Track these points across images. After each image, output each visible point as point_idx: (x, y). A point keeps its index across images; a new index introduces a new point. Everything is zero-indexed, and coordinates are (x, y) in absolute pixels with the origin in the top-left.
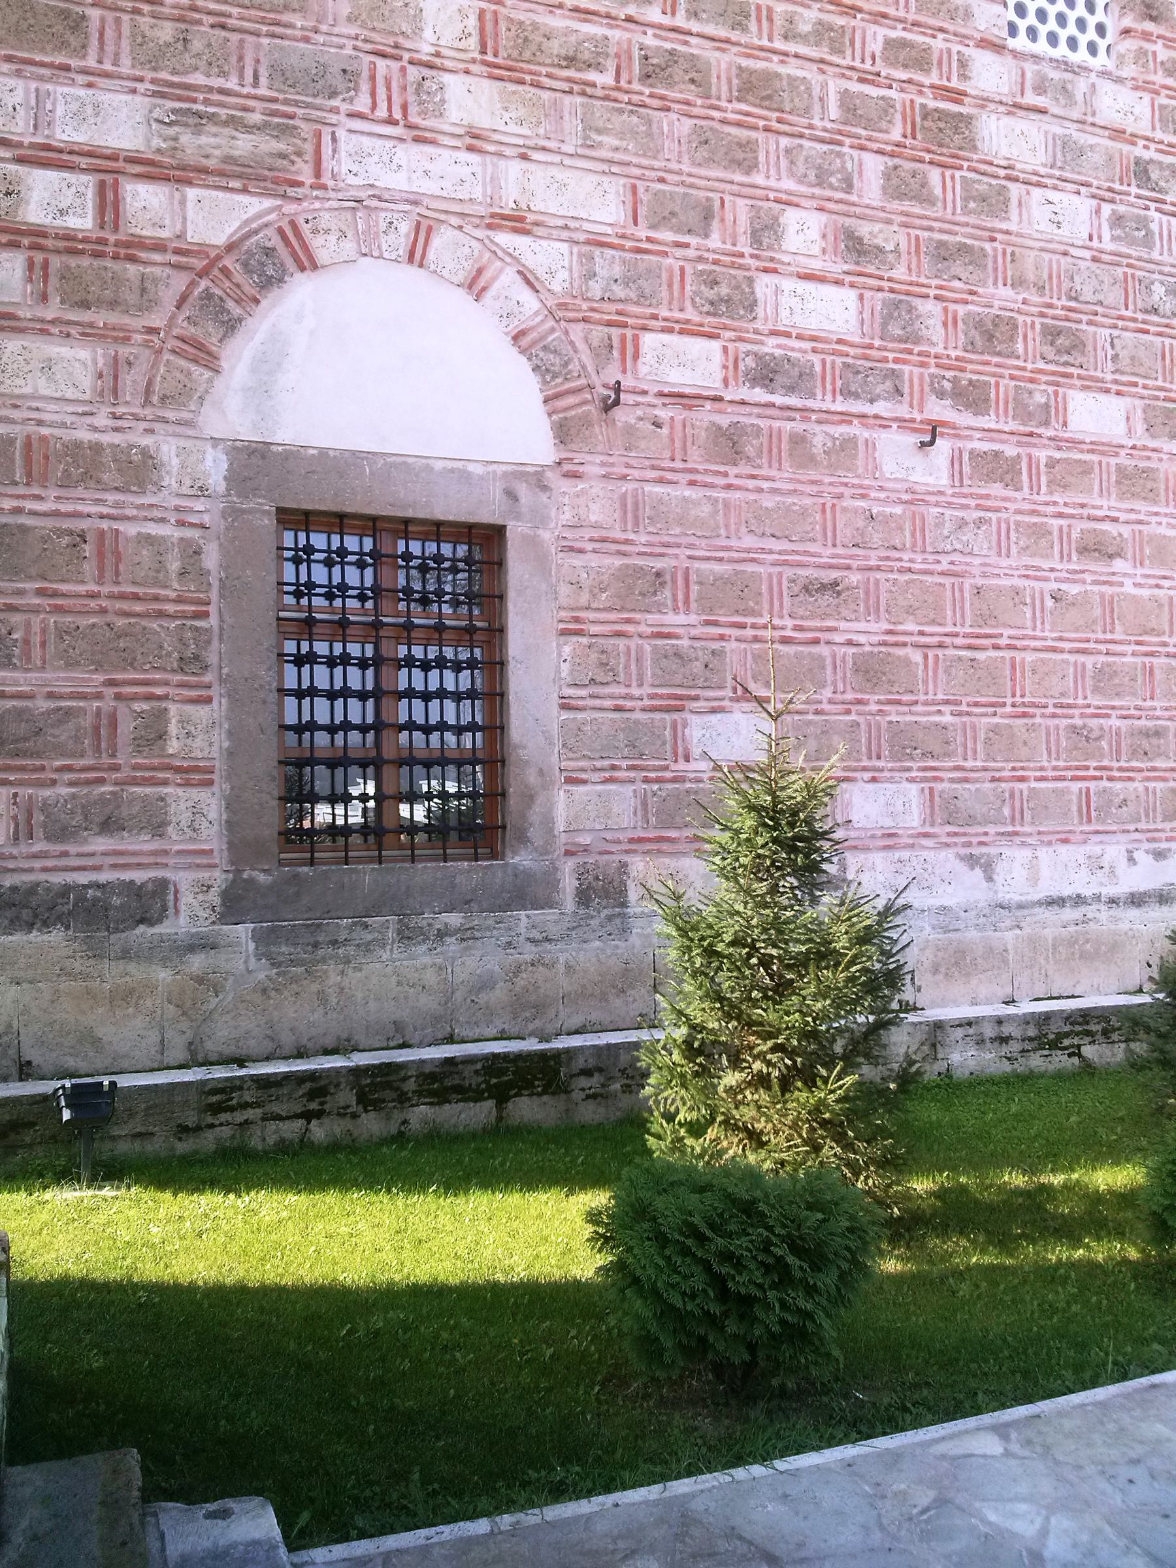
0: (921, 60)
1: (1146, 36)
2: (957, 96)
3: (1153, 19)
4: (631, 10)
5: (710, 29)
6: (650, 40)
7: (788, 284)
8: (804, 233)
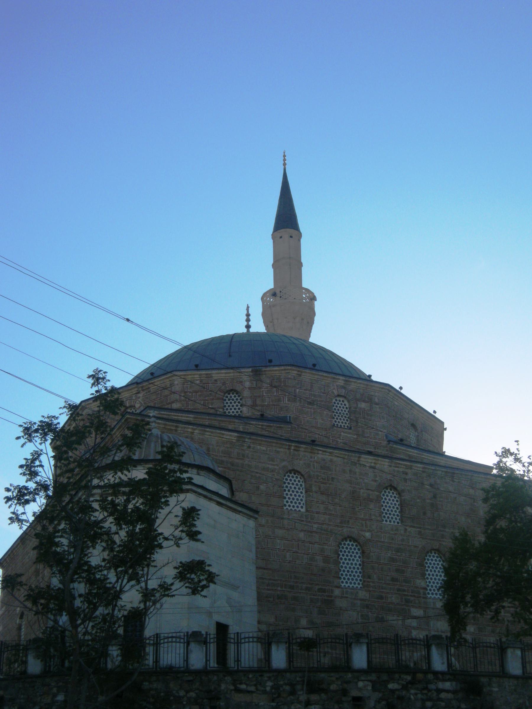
0: (324, 591)
1: (368, 582)
2: (331, 596)
3: (370, 578)
4: (276, 588)
5: (288, 590)
6: (279, 593)
7: (301, 630)
8: (304, 622)
